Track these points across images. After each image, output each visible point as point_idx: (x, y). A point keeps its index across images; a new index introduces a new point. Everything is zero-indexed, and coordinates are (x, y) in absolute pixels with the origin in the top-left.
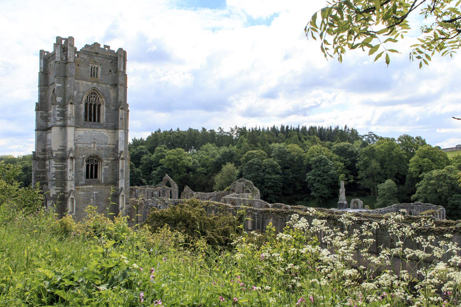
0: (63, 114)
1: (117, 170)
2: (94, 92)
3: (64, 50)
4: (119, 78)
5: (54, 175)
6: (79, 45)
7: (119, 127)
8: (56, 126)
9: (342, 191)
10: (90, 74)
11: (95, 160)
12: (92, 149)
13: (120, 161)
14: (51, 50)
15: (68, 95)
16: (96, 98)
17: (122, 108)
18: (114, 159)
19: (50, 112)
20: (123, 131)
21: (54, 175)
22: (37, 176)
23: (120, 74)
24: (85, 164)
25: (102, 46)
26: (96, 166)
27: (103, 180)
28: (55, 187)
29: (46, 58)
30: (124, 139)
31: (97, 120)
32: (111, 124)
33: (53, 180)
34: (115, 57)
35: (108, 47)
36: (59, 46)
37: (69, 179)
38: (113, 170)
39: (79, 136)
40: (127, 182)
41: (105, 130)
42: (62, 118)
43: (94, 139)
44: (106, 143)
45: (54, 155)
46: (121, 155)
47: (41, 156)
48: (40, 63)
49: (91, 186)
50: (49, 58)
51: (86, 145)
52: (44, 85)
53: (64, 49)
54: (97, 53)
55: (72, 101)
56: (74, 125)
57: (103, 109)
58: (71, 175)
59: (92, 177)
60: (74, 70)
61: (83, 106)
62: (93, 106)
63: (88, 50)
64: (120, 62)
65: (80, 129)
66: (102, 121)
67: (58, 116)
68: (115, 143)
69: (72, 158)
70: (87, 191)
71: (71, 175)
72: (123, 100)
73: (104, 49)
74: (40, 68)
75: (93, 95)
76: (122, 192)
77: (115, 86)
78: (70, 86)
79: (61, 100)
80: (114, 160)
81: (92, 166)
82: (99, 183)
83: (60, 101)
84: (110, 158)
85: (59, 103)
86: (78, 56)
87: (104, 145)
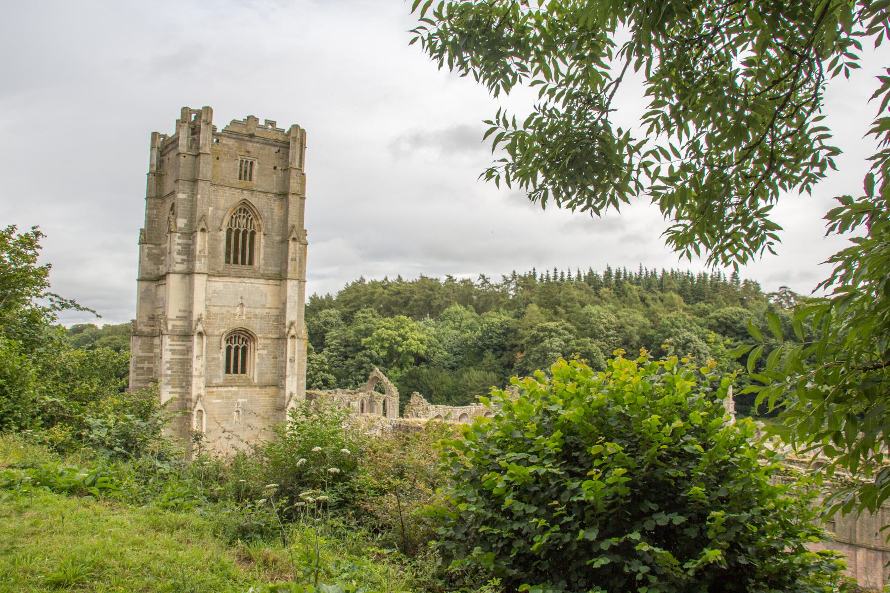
0: (189, 252)
1: (284, 359)
2: (245, 208)
3: (195, 131)
4: (292, 181)
5: (168, 365)
6: (220, 122)
7: (289, 276)
8: (174, 273)
9: (729, 404)
10: (238, 174)
11: (243, 339)
12: (237, 317)
13: (289, 340)
14: (171, 132)
15: (198, 215)
16: (247, 219)
17: (294, 239)
18: (277, 336)
19: (163, 246)
20: (296, 282)
21: (168, 365)
22: (139, 365)
23: (293, 173)
24: (224, 345)
25: (262, 123)
26: (244, 350)
27: (256, 377)
28: (169, 388)
29: (164, 148)
30: (296, 298)
31: (247, 262)
32: (273, 269)
33: (166, 375)
34: (283, 142)
35: (273, 123)
36: (186, 124)
37: (195, 373)
38: (275, 358)
39: (214, 292)
40: (301, 382)
41: (262, 281)
42: (185, 257)
43: (242, 298)
44: (263, 306)
45: (170, 327)
46: (290, 329)
47: (146, 330)
48: (151, 156)
49: (235, 389)
50: (166, 147)
51: (227, 309)
52: (157, 197)
53: (193, 129)
54: (252, 136)
55: (203, 226)
56: (205, 271)
57: (260, 241)
58: (199, 367)
59: (236, 372)
60: (210, 167)
61: (223, 235)
62: (241, 235)
63: (236, 129)
64: (294, 152)
65: (217, 279)
66: (256, 264)
67: (178, 254)
68: (281, 306)
69: (200, 334)
70: (227, 398)
71: (199, 367)
72: (296, 224)
73: (264, 128)
74: (151, 166)
75: (242, 215)
76: (292, 401)
77: (283, 195)
78: (202, 197)
79: (186, 225)
80: (278, 339)
81: (237, 348)
82: (249, 384)
83: (183, 226)
84: (270, 336)
85: (180, 229)
86: (218, 141)
87: (259, 310)
